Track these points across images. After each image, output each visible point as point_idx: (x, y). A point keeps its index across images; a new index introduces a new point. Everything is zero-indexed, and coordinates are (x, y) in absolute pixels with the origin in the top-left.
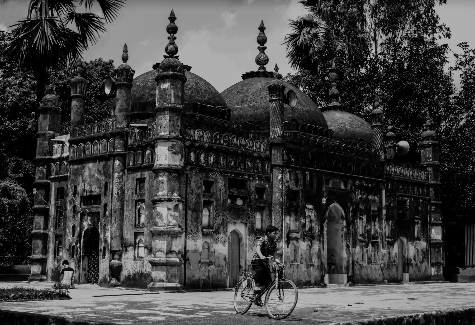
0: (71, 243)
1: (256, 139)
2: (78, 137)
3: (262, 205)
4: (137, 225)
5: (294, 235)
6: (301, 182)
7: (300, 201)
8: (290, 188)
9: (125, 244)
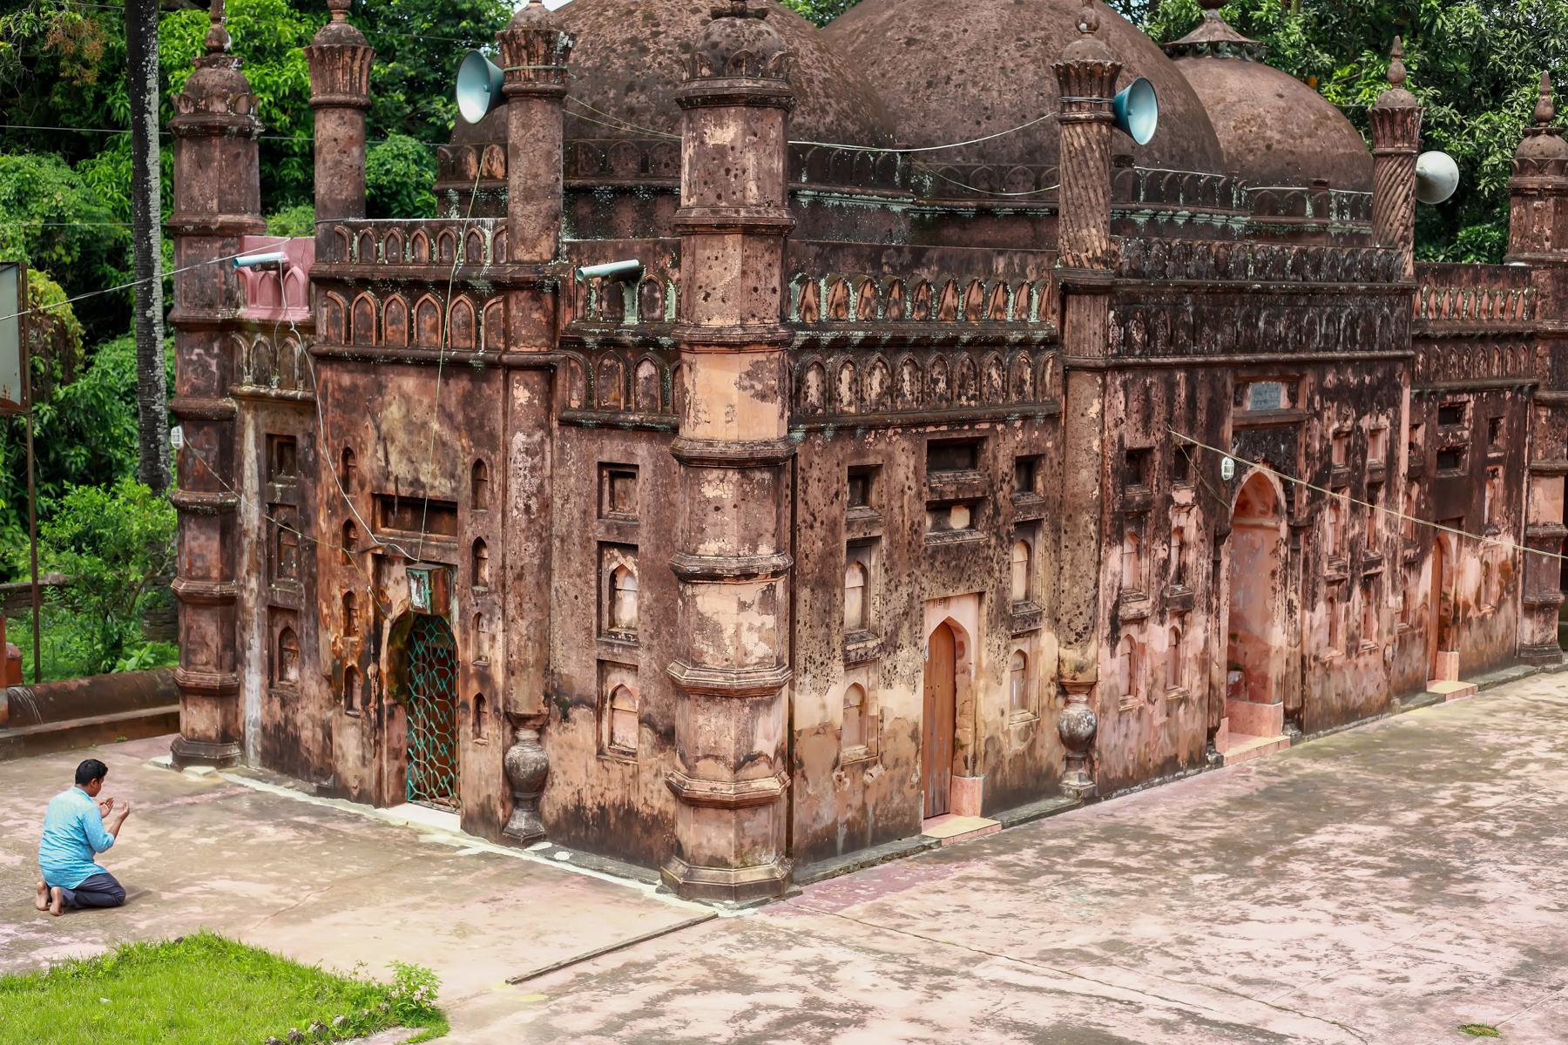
0: (343, 660)
1: (1014, 275)
2: (352, 268)
3: (1031, 517)
4: (604, 628)
5: (1131, 609)
6: (1160, 414)
8: (1127, 443)
9: (556, 691)
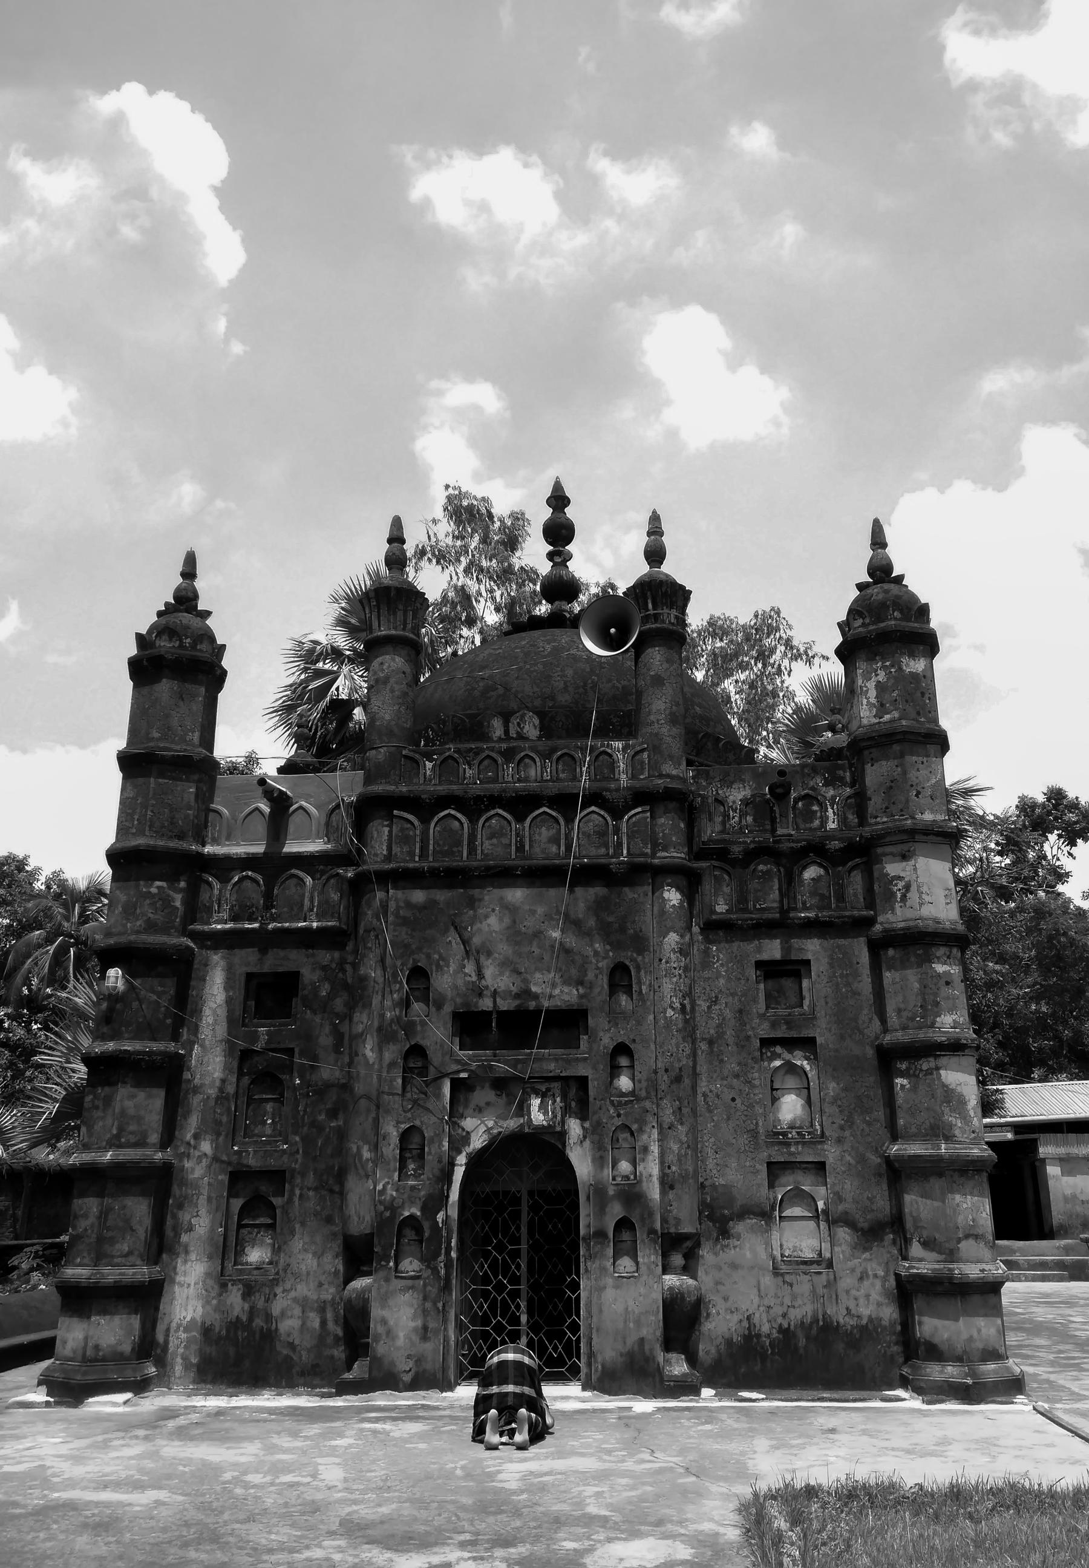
9: (710, 1207)
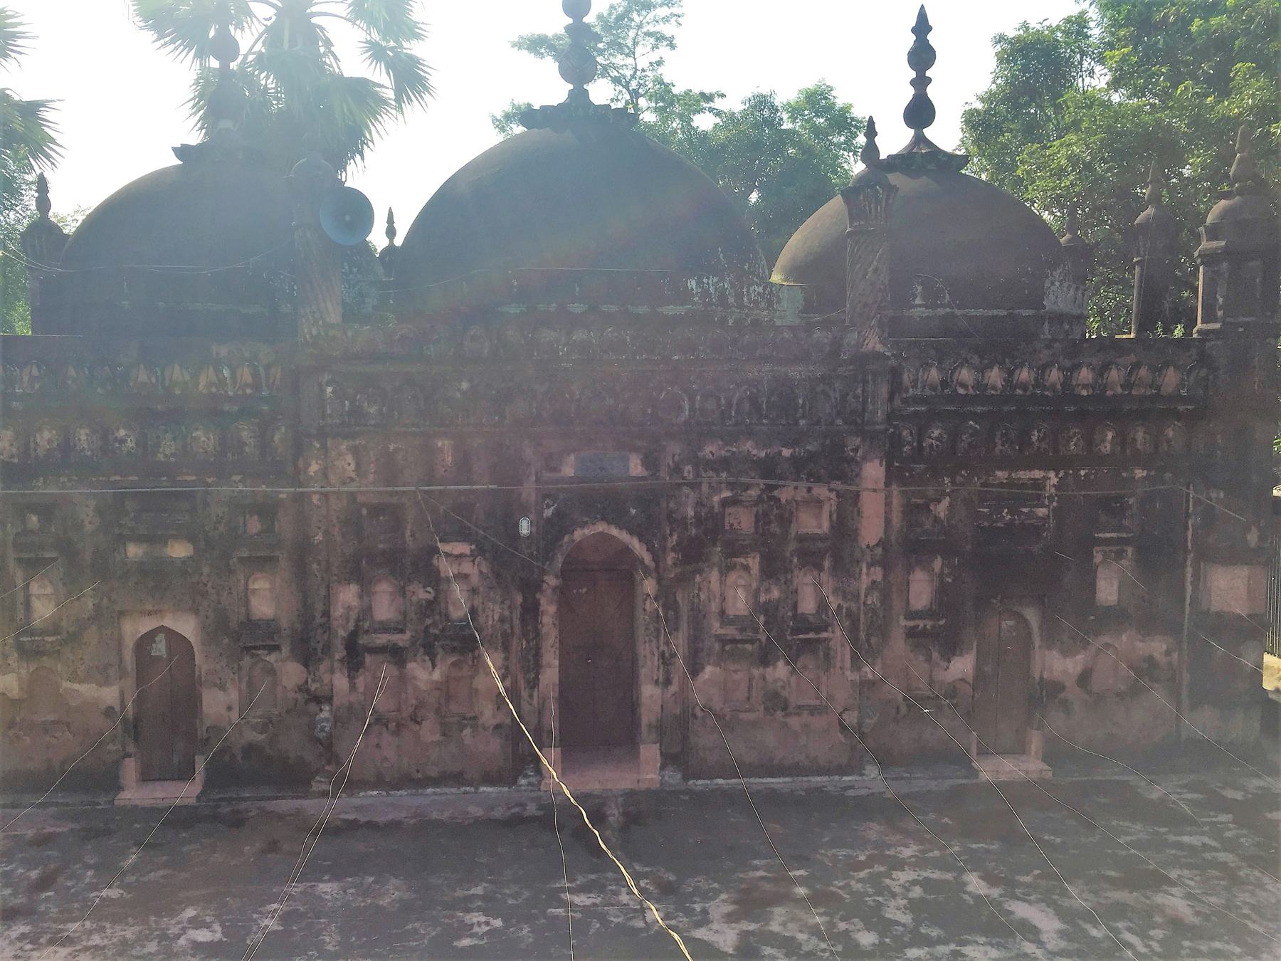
5: (382, 639)
7: (408, 533)
